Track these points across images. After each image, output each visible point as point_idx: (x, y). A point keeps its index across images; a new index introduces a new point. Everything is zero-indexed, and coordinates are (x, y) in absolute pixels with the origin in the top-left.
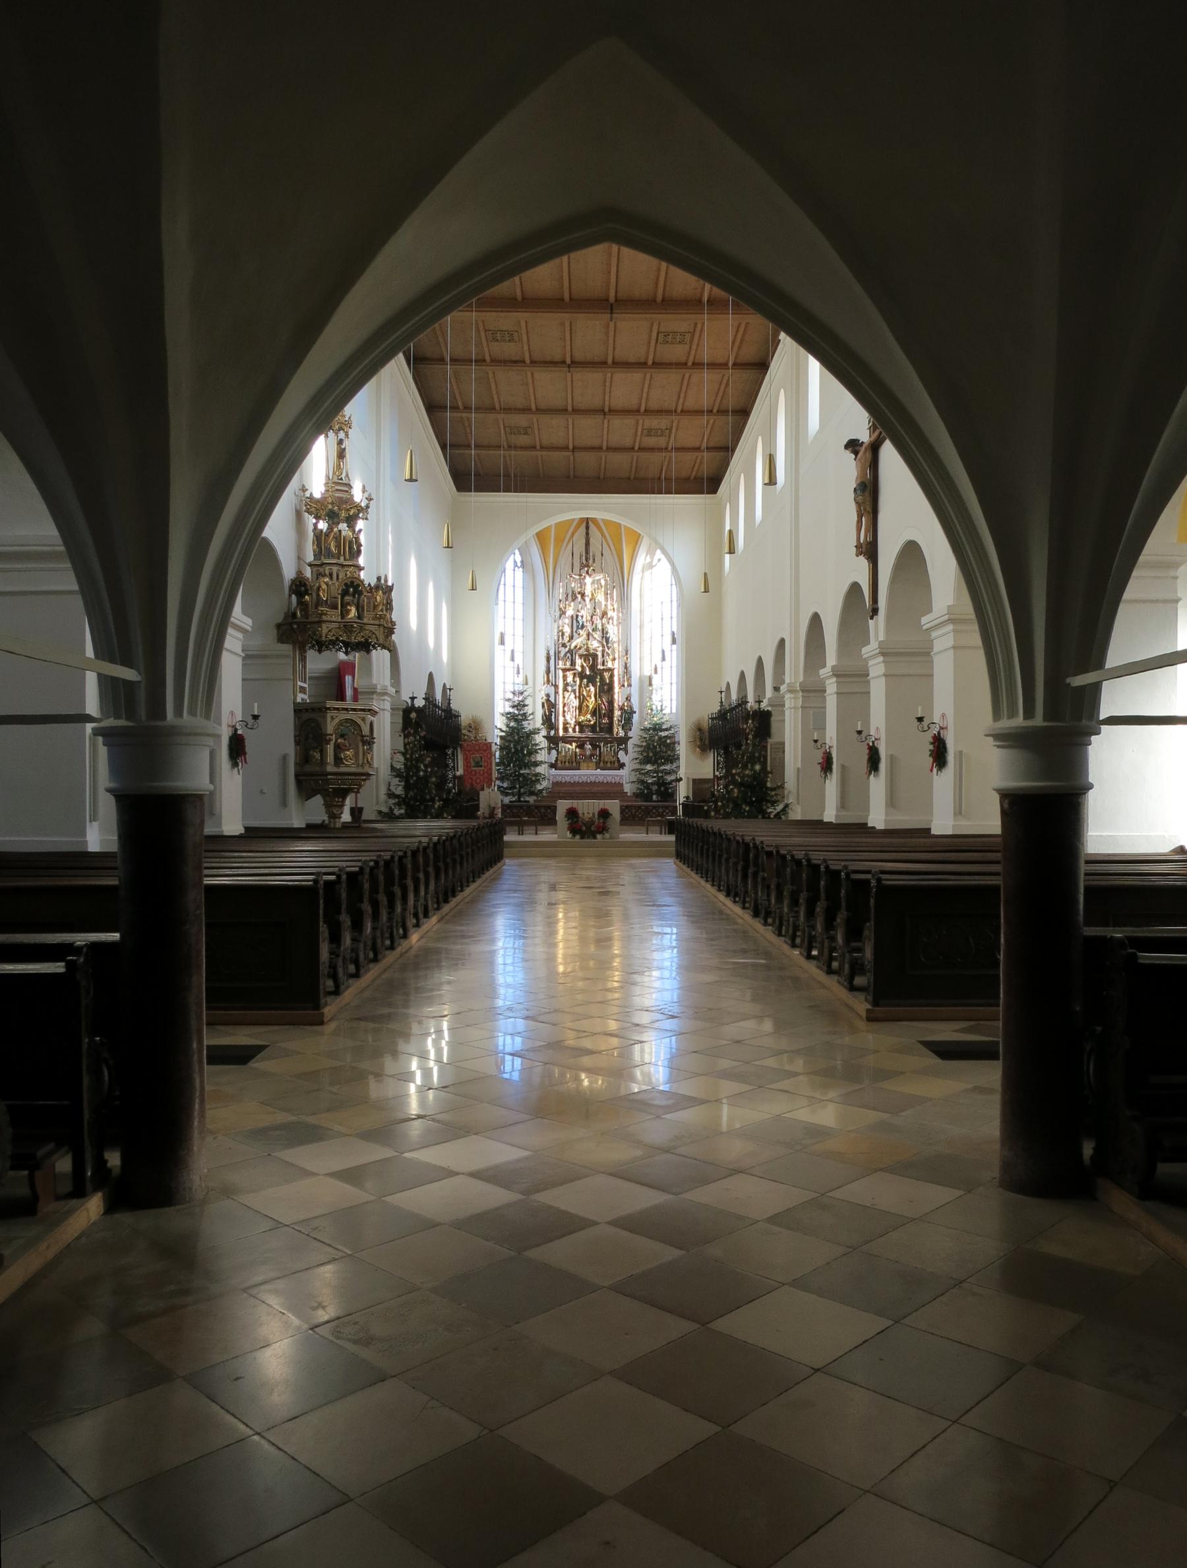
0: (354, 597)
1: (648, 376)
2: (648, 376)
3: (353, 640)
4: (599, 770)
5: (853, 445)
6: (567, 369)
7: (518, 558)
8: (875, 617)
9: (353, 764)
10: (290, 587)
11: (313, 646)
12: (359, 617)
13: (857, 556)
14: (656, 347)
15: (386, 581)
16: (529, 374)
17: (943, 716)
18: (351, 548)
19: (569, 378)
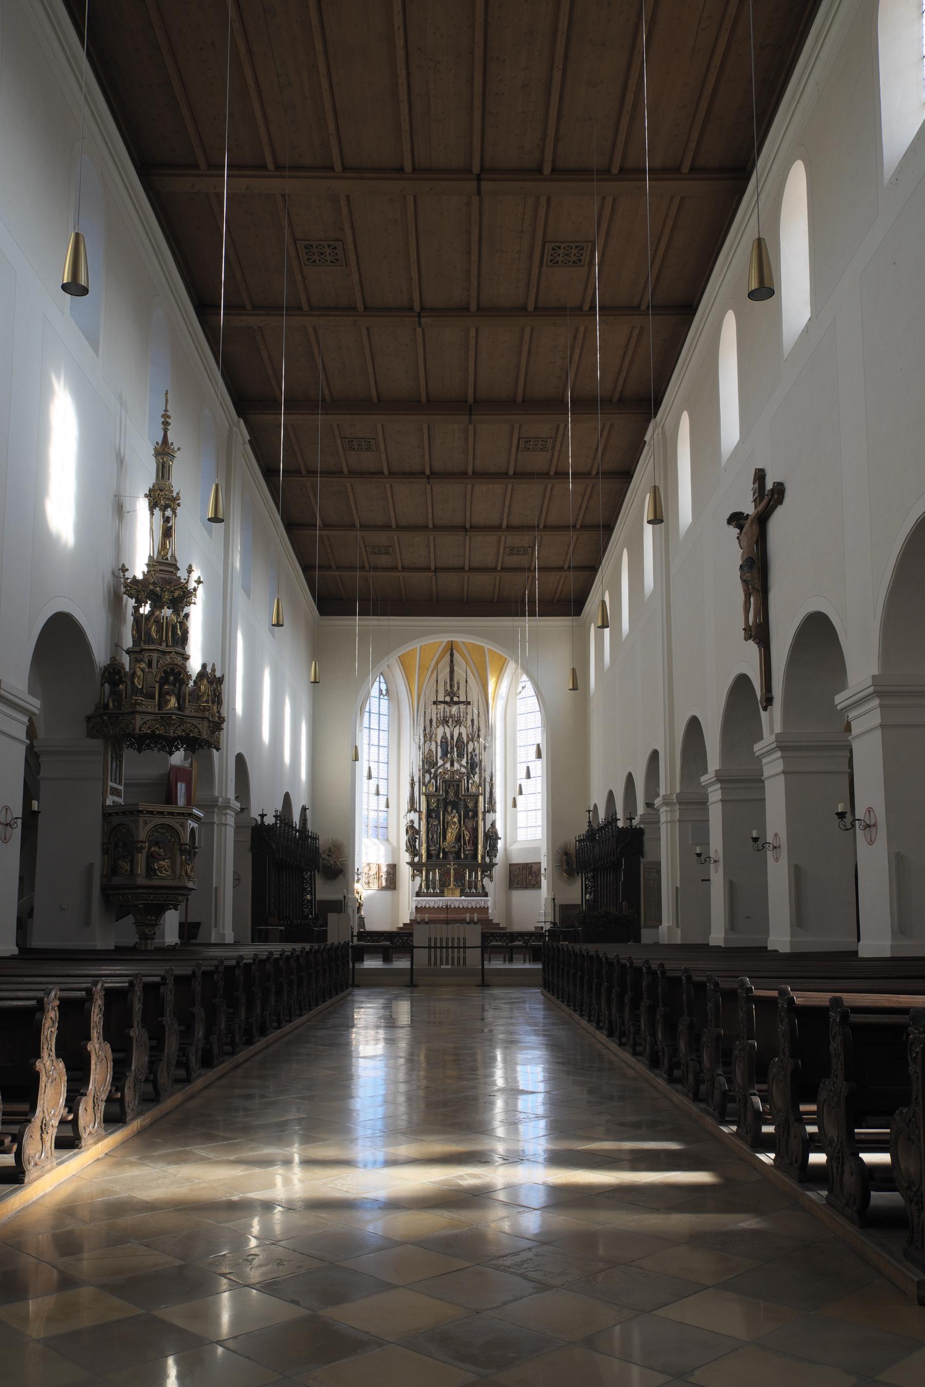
0: (175, 686)
1: (510, 487)
2: (510, 487)
3: (172, 734)
4: (463, 898)
5: (736, 519)
6: (426, 480)
7: (383, 687)
8: (769, 707)
9: (168, 876)
10: (103, 675)
11: (131, 746)
12: (180, 708)
13: (746, 640)
14: (517, 454)
15: (213, 670)
16: (388, 486)
17: (869, 810)
18: (174, 633)
19: (429, 491)
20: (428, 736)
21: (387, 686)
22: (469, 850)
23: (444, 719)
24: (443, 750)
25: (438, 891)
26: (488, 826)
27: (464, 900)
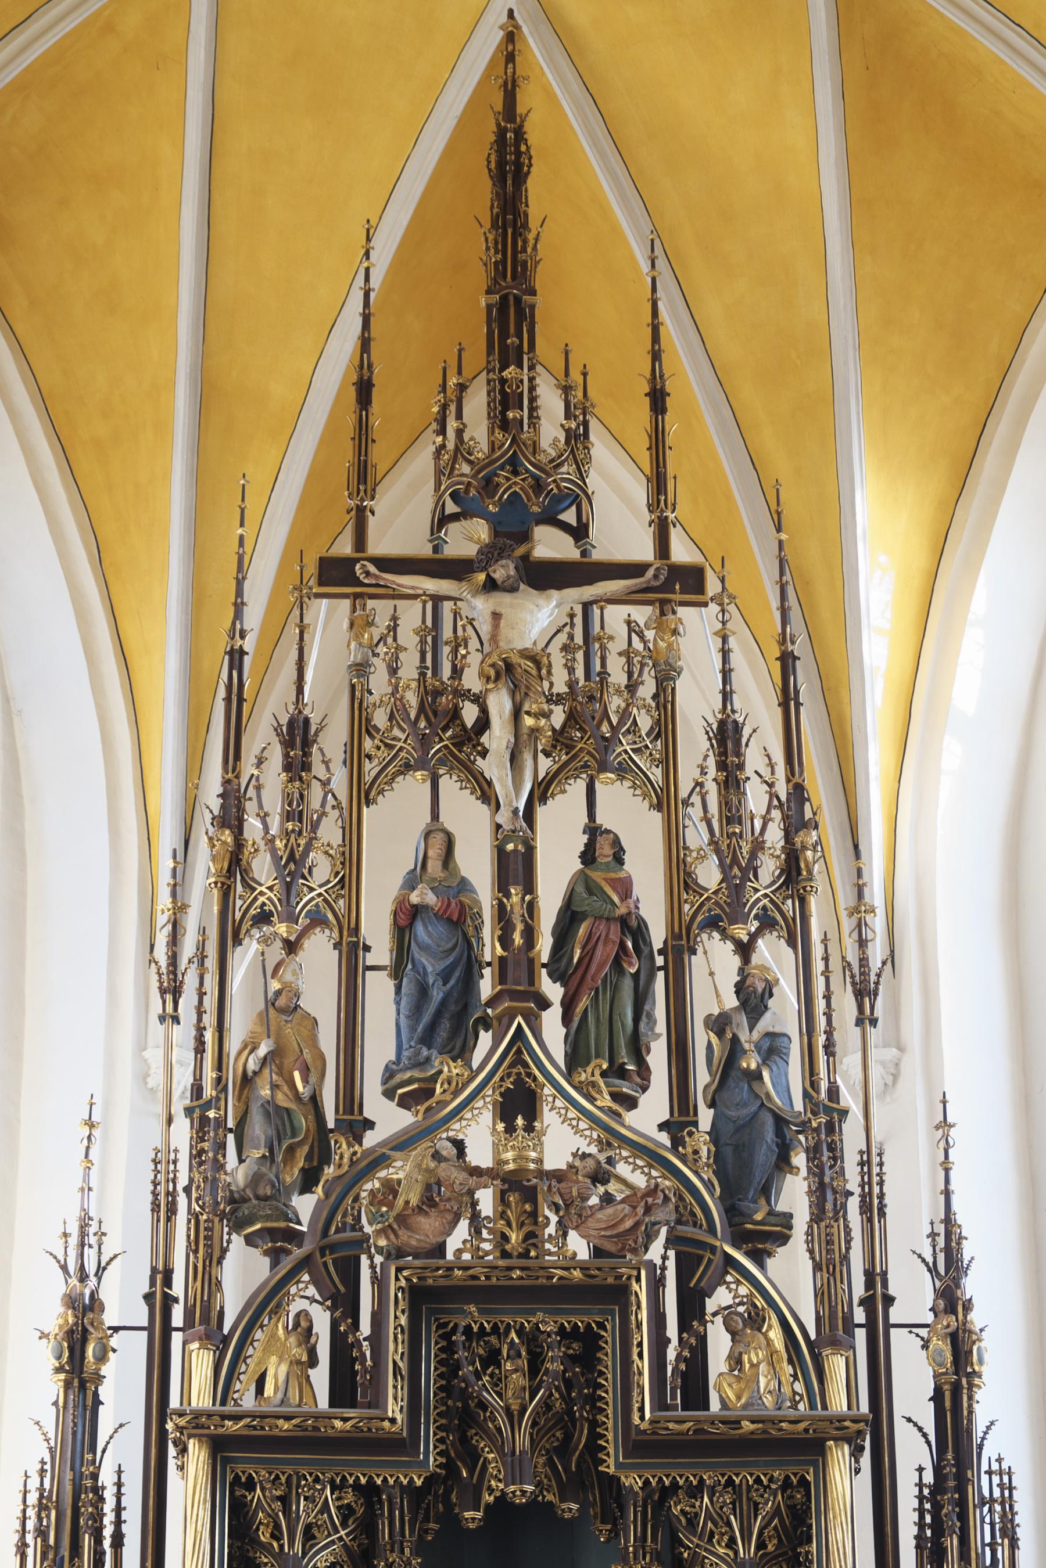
23: (430, 695)
24: (423, 991)
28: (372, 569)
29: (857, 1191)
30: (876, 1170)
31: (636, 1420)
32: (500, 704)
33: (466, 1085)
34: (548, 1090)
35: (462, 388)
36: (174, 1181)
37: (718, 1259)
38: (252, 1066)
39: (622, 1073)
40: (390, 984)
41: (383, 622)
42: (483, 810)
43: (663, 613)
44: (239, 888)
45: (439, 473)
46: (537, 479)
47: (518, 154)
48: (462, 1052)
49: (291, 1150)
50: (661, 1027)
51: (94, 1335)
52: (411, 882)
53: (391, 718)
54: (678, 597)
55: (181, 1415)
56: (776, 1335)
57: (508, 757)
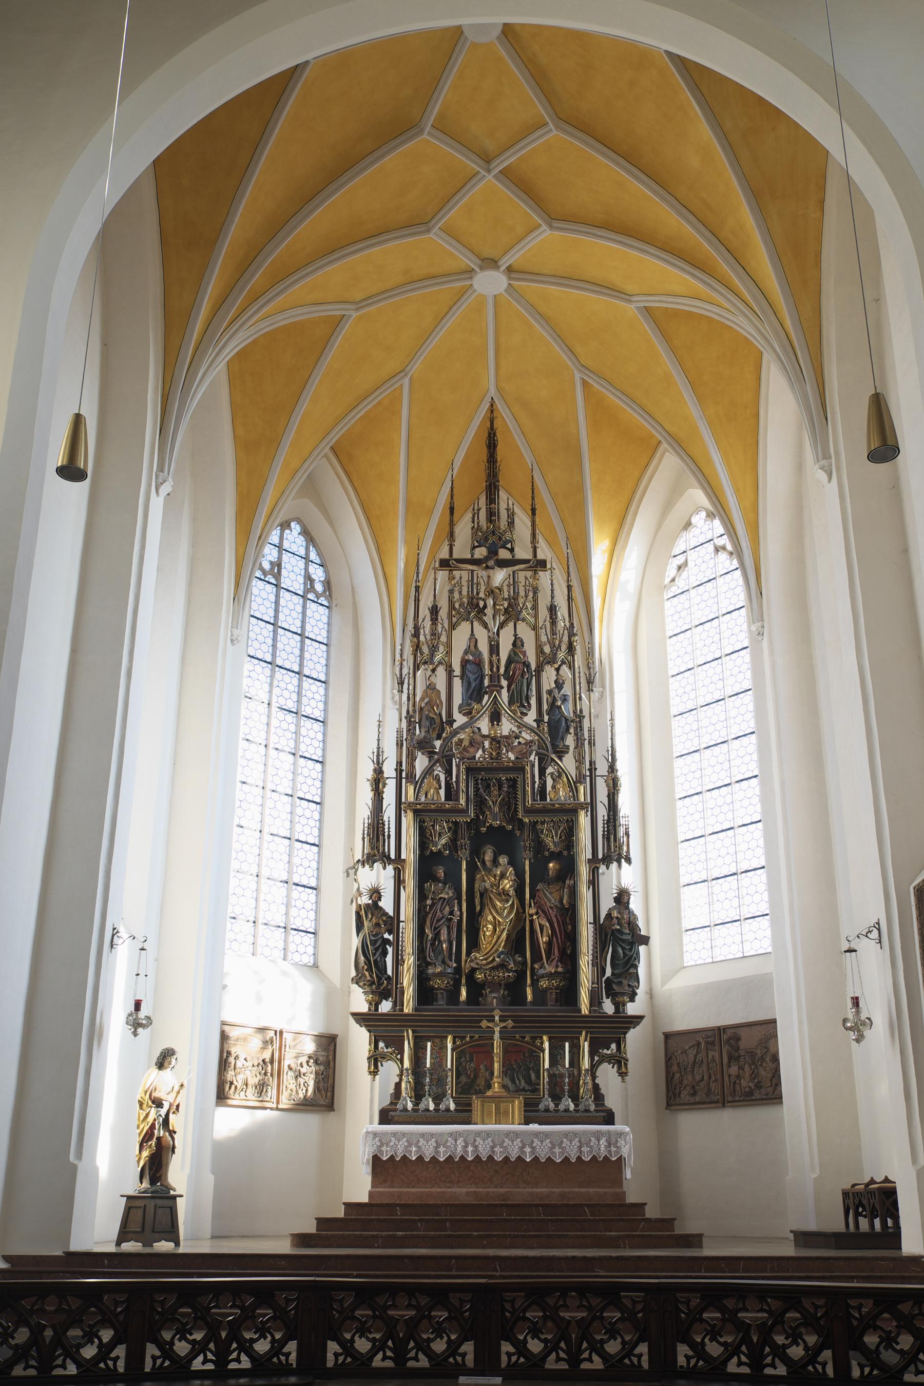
4: (534, 1127)
7: (318, 574)
20: (425, 650)
21: (326, 572)
22: (550, 976)
24: (469, 684)
25: (452, 1107)
26: (607, 903)
27: (537, 1134)
28: (455, 563)
29: (587, 738)
30: (592, 732)
31: (527, 804)
32: (490, 602)
33: (481, 711)
34: (503, 712)
35: (479, 510)
36: (402, 737)
37: (550, 759)
38: (423, 705)
39: (524, 707)
40: (460, 681)
41: (458, 578)
42: (486, 631)
43: (535, 574)
44: (419, 654)
45: (472, 534)
46: (500, 537)
47: (494, 440)
48: (479, 701)
49: (434, 729)
50: (534, 693)
51: (382, 780)
52: (466, 652)
53: (460, 605)
54: (539, 569)
55: (405, 804)
56: (565, 779)
57: (492, 617)
